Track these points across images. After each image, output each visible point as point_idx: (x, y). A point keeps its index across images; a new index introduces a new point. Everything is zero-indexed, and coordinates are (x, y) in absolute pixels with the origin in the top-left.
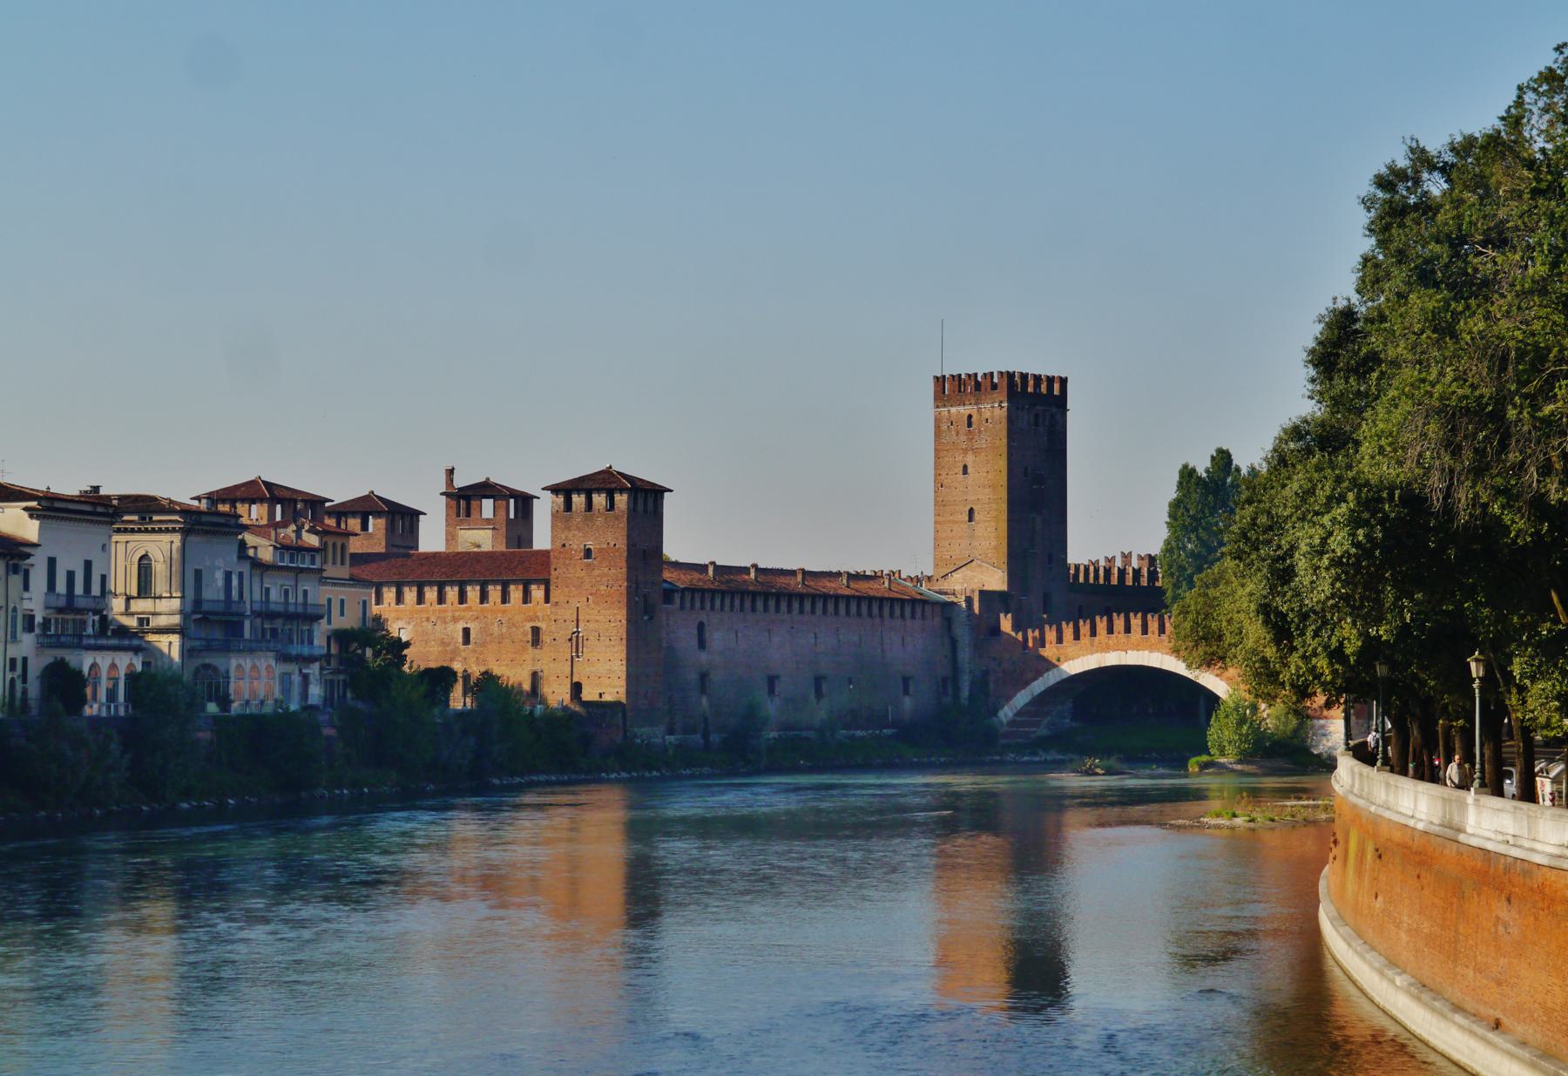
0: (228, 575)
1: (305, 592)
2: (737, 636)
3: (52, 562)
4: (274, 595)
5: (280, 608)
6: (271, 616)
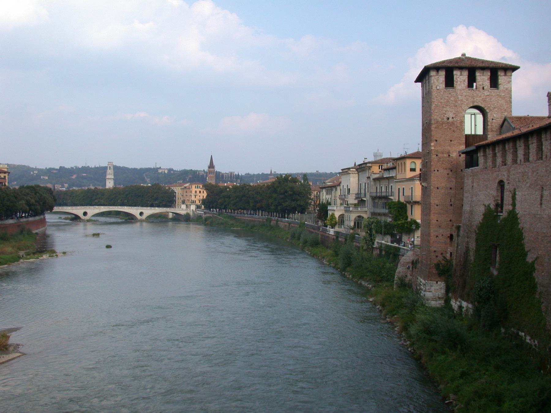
0: (365, 183)
1: (392, 186)
2: (542, 197)
3: (343, 186)
4: (383, 190)
5: (384, 194)
6: (380, 198)
